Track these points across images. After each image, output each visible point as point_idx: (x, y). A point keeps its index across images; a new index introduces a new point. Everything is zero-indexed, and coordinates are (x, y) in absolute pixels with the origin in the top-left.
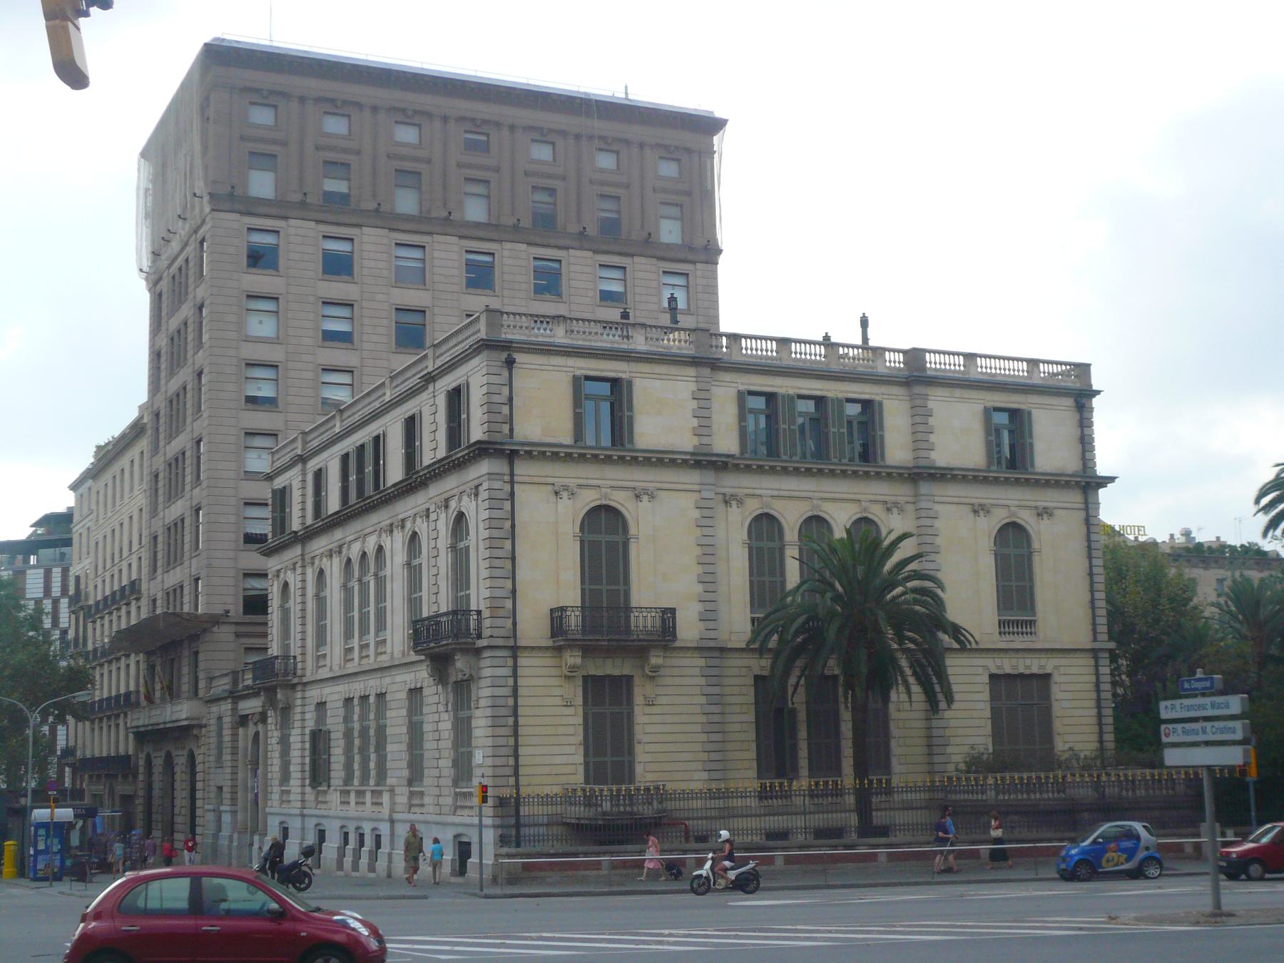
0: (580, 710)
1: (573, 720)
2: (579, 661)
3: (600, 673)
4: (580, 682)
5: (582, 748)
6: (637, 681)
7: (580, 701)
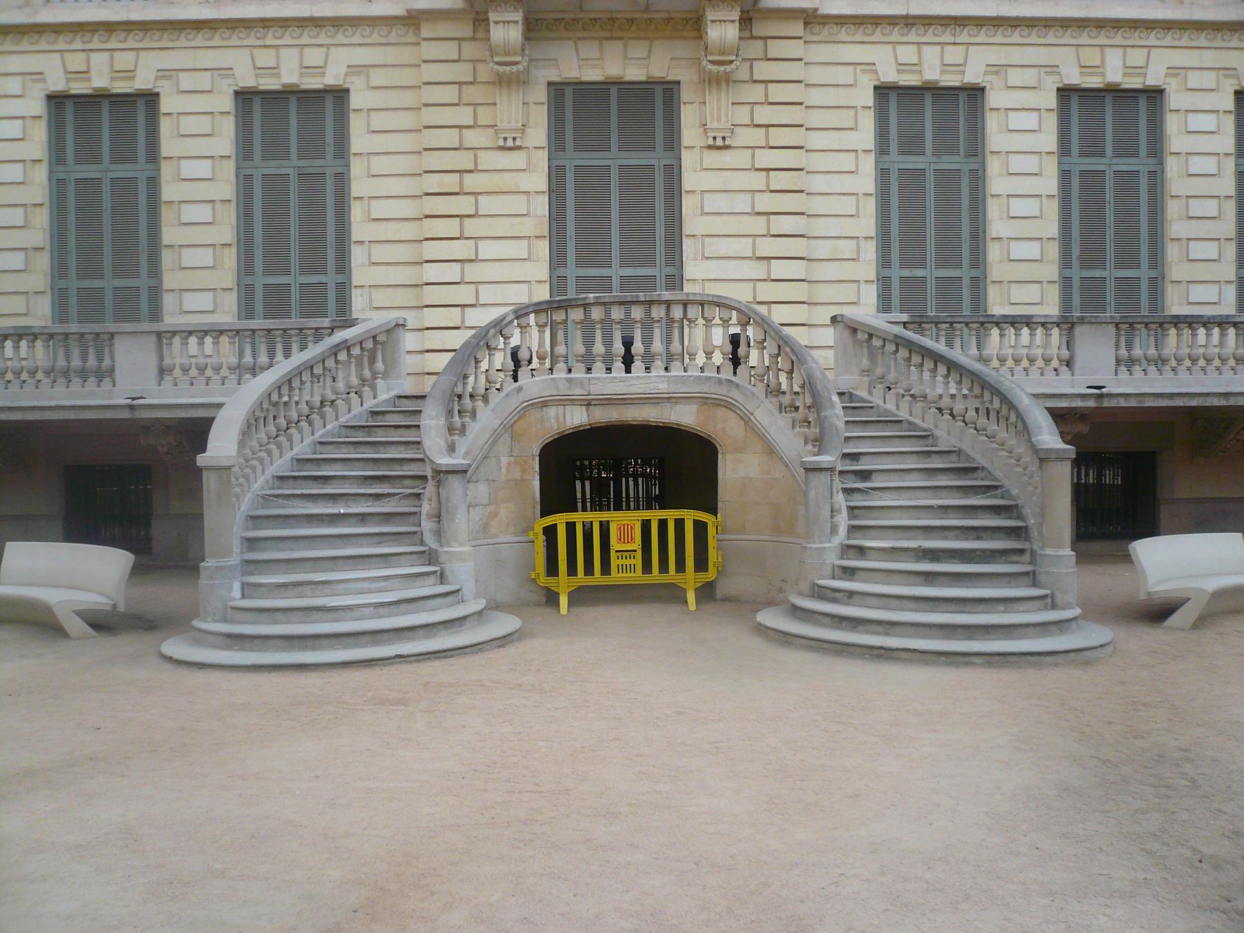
0: (542, 159)
1: (518, 184)
2: (514, 34)
3: (593, 75)
4: (541, 94)
5: (543, 248)
6: (686, 94)
7: (538, 135)
